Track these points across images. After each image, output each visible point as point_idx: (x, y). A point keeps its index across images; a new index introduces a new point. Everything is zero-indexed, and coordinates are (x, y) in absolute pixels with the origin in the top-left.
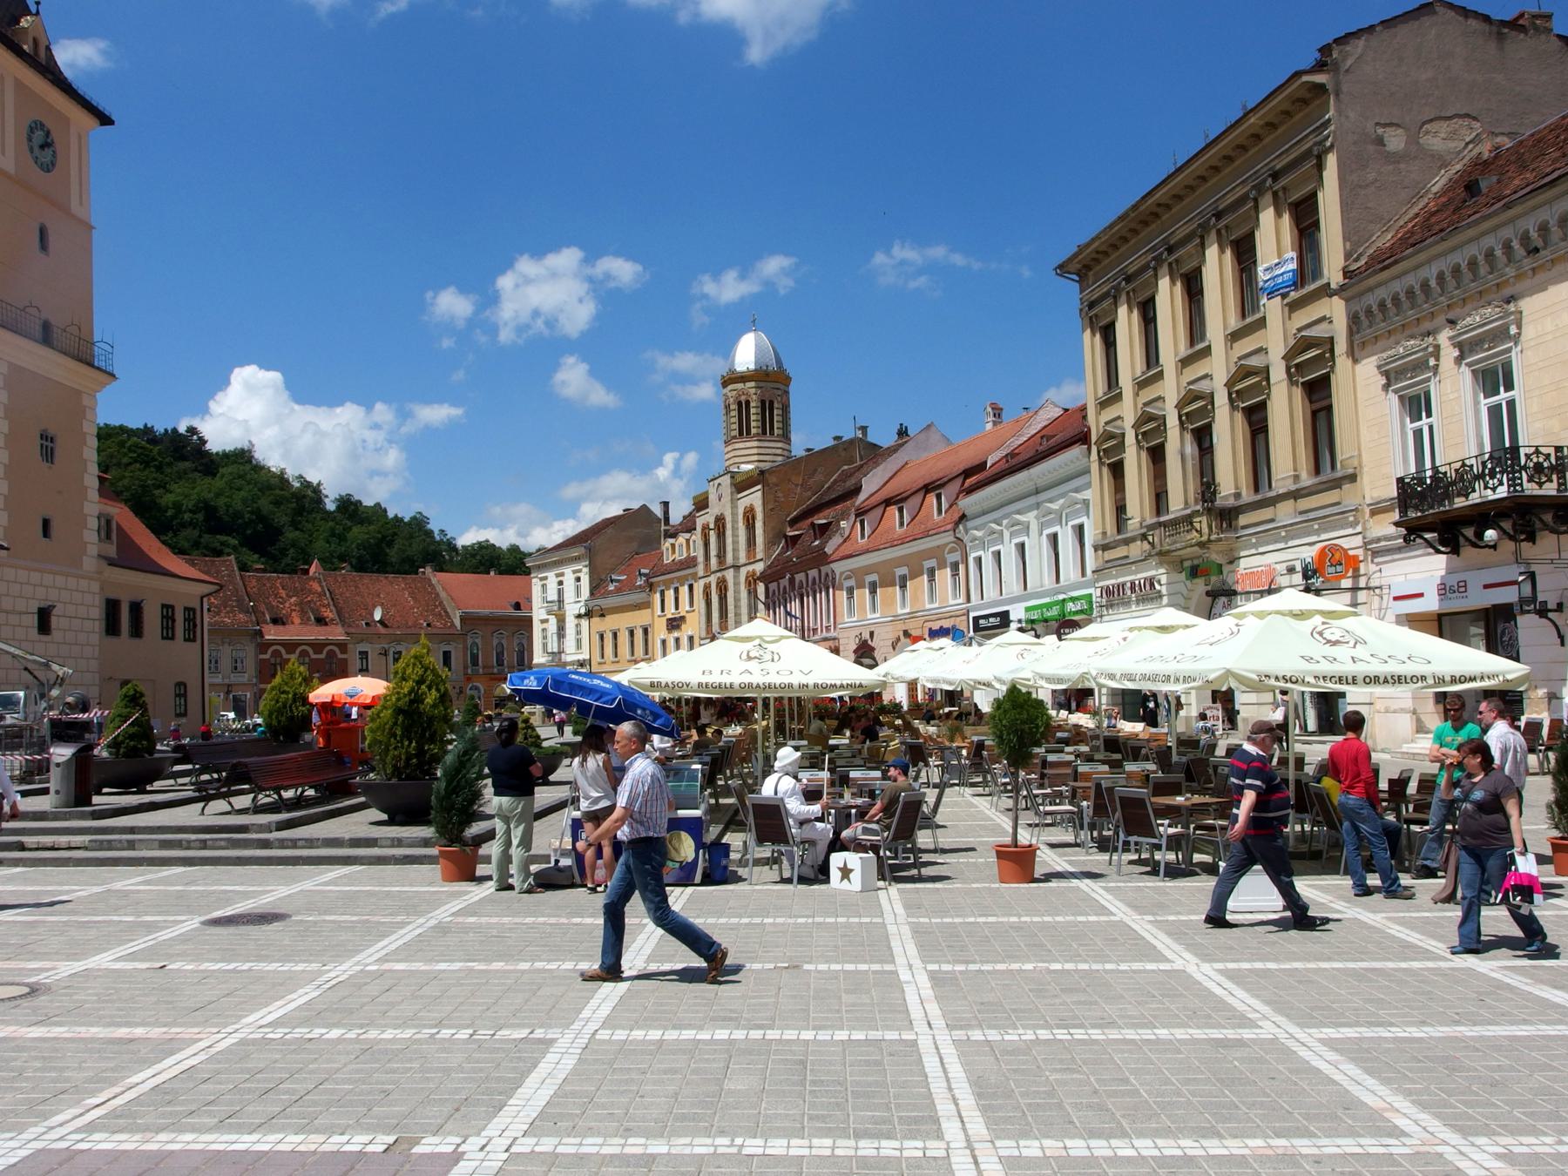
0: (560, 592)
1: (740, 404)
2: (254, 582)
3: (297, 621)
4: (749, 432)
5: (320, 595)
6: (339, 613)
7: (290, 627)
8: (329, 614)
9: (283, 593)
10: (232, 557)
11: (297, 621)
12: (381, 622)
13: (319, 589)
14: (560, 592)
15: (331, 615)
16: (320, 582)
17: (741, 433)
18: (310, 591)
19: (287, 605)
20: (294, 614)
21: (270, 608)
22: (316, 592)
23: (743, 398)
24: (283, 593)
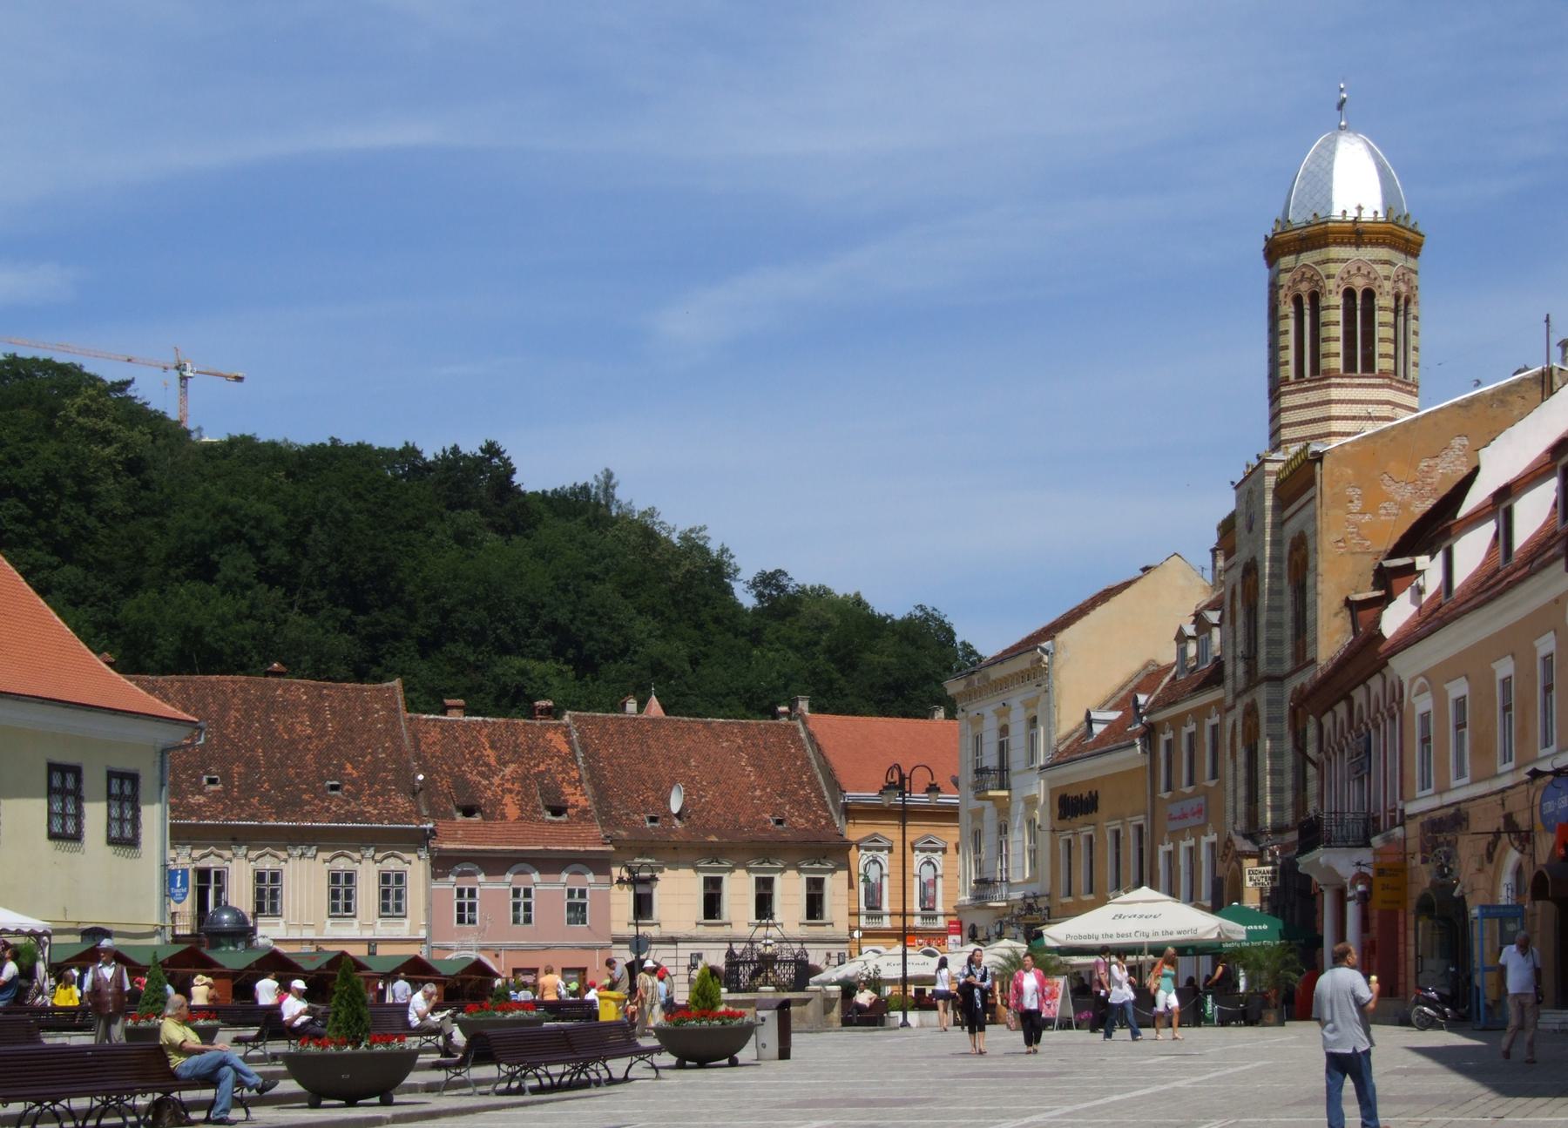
0: (1003, 748)
1: (1349, 294)
2: (435, 734)
3: (512, 811)
4: (1369, 366)
5: (564, 760)
6: (601, 794)
7: (498, 826)
8: (578, 798)
9: (491, 756)
10: (397, 683)
11: (512, 811)
12: (678, 816)
13: (565, 749)
14: (1003, 748)
15: (582, 802)
16: (567, 734)
17: (1350, 366)
18: (548, 752)
19: (496, 780)
20: (507, 799)
21: (461, 784)
22: (558, 753)
23: (1359, 284)
24: (491, 756)
